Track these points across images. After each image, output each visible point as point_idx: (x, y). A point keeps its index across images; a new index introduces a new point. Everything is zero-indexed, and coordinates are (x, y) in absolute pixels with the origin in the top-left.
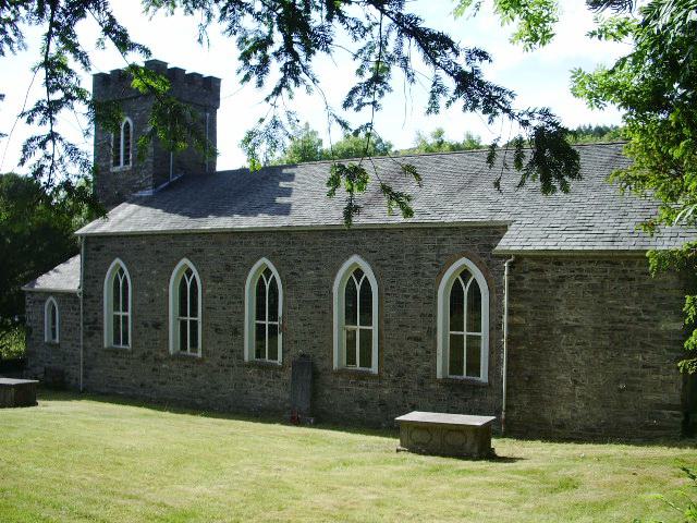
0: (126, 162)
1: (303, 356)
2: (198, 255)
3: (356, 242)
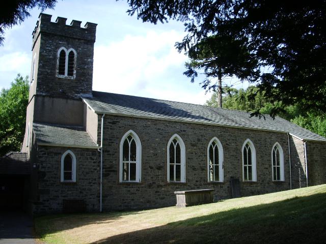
0: (70, 73)
1: (231, 177)
2: (183, 133)
3: (248, 134)
